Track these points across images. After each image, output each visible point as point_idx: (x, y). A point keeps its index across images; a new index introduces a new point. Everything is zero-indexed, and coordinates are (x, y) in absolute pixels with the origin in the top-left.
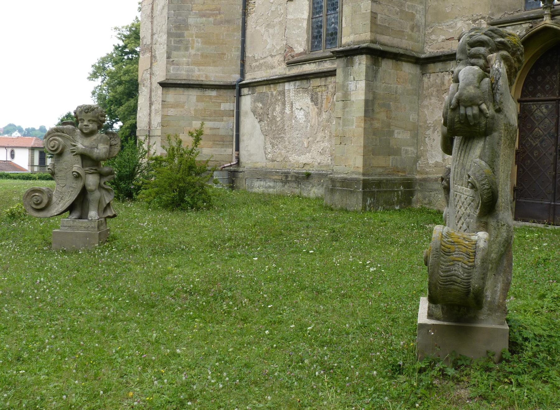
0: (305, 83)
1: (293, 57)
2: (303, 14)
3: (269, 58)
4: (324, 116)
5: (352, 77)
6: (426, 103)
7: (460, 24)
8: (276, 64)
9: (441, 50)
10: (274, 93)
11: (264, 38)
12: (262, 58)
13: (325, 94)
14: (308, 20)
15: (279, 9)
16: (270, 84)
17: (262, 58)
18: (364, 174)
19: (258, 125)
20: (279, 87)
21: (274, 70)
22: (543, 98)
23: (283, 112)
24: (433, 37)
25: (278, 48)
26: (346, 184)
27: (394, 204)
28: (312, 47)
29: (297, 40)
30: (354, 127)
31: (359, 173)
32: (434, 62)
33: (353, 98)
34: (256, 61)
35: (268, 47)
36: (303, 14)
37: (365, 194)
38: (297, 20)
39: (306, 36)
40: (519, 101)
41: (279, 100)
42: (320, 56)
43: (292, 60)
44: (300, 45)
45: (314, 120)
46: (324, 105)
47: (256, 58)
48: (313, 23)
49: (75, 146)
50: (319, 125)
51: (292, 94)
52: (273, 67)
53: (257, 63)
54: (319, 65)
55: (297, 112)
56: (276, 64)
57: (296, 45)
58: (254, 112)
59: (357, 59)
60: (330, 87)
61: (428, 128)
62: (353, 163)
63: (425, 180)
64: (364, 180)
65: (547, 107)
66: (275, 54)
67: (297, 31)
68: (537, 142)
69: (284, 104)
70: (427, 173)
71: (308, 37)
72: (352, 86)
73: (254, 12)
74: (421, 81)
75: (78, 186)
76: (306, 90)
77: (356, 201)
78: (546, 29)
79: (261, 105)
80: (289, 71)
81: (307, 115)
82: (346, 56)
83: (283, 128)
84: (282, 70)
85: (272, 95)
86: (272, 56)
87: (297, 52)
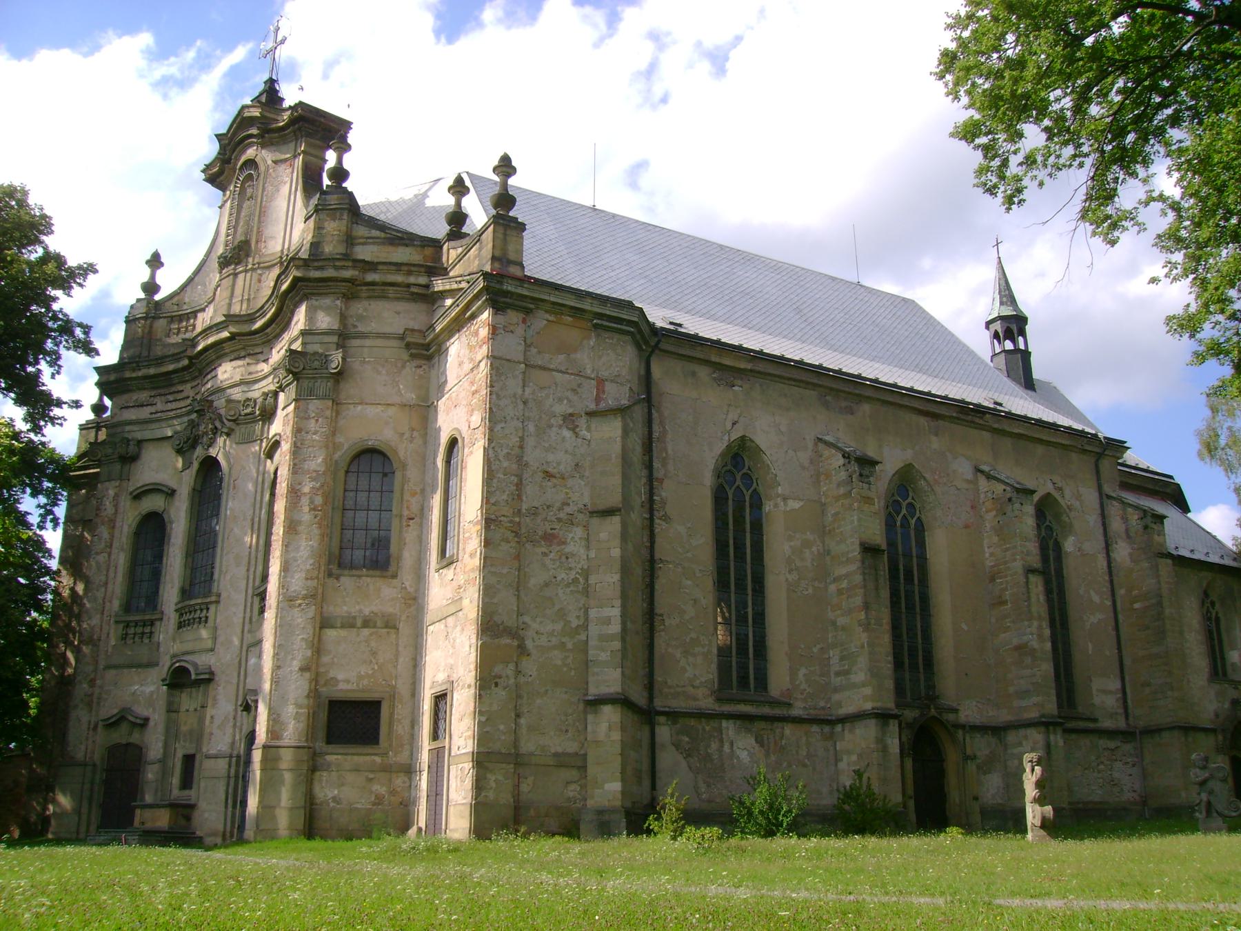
4: (773, 758)
10: (707, 728)
19: (684, 764)
20: (714, 723)
23: (720, 749)
25: (703, 680)
33: (891, 751)
55: (738, 752)
58: (677, 746)
59: (891, 721)
69: (721, 741)
72: (889, 741)
76: (748, 731)
81: (751, 755)
85: (704, 729)
86: (694, 687)
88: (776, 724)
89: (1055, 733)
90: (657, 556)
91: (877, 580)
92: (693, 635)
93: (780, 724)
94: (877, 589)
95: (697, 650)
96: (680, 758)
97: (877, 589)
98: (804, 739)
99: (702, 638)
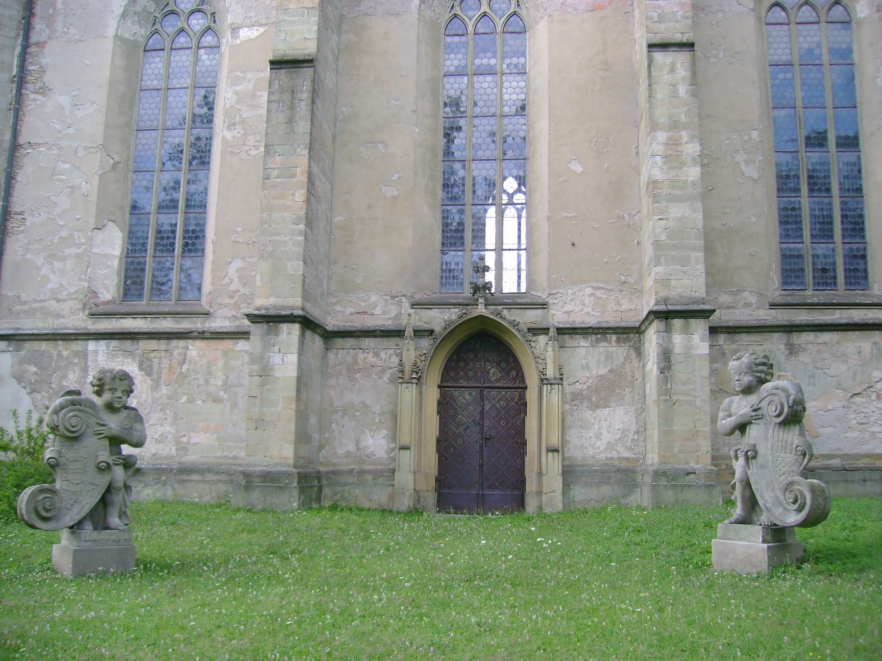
0: (128, 344)
1: (97, 305)
2: (114, 249)
3: (53, 303)
4: (164, 390)
5: (276, 348)
6: (332, 382)
7: (374, 298)
8: (67, 311)
9: (350, 324)
11: (43, 272)
12: (35, 301)
13: (166, 362)
14: (121, 259)
15: (76, 237)
16: (56, 340)
17: (35, 301)
18: (295, 466)
20: (78, 346)
21: (61, 320)
22: (465, 384)
24: (338, 308)
25: (73, 290)
26: (271, 479)
27: (657, 474)
28: (125, 295)
29: (104, 284)
30: (280, 409)
31: (288, 466)
32: (343, 337)
33: (278, 374)
34: (25, 303)
35: (50, 286)
36: (114, 249)
37: (302, 490)
38: (105, 256)
39: (116, 280)
40: (439, 387)
41: (75, 364)
42: (140, 310)
43: (95, 309)
44: (109, 290)
45: (144, 396)
46: (163, 376)
47: (23, 299)
49: (104, 425)
50: (153, 402)
51: (100, 358)
52: (58, 316)
53: (26, 307)
54: (151, 322)
56: (67, 311)
58: (19, 378)
59: (285, 327)
60: (176, 352)
61: (336, 412)
62: (280, 451)
63: (334, 472)
64: (299, 473)
65: (470, 394)
66: (65, 297)
67: (104, 272)
68: (461, 429)
70: (334, 465)
71: (120, 281)
72: (276, 358)
73: (23, 232)
74: (325, 357)
75: (103, 481)
77: (292, 499)
78: (481, 318)
79: (35, 369)
80: (93, 324)
82: (268, 322)
84: (79, 321)
85: (60, 355)
86: (58, 300)
88: (174, 343)
89: (686, 331)
90: (22, 139)
91: (292, 107)
92: (64, 233)
93: (182, 343)
94: (290, 121)
95: (68, 251)
96: (23, 394)
97: (290, 121)
98: (221, 363)
99: (76, 234)
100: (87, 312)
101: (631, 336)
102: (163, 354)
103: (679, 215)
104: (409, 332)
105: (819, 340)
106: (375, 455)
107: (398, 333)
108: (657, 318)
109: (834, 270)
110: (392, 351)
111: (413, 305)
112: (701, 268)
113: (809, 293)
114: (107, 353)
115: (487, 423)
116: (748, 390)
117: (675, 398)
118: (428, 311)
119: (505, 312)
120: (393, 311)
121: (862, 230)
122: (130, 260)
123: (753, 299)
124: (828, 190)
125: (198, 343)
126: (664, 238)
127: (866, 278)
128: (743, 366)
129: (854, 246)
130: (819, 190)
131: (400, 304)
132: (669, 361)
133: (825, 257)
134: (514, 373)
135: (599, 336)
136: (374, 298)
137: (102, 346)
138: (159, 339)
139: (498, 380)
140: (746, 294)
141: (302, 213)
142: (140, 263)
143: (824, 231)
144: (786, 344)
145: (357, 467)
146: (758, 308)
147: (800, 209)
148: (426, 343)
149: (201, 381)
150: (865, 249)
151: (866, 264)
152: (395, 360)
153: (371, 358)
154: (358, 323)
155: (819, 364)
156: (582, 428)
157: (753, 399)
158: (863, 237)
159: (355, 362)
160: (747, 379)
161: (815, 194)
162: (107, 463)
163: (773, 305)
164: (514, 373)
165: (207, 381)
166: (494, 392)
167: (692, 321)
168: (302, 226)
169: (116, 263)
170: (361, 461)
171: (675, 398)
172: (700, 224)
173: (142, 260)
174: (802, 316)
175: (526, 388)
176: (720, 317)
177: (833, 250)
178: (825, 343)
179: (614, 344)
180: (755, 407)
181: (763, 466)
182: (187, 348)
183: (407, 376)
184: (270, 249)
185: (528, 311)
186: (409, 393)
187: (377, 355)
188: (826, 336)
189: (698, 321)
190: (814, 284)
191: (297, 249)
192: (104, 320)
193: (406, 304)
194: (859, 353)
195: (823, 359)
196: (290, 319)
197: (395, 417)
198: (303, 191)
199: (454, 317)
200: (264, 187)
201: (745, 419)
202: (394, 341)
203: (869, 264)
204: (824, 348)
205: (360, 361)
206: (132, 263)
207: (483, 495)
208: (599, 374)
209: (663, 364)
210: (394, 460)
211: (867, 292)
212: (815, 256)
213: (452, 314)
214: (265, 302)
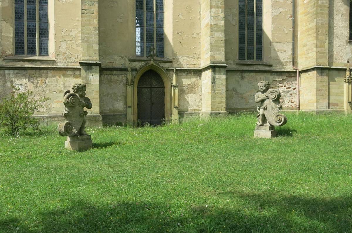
1: (6, 56)
2: (10, 34)
9: (108, 66)
14: (13, 38)
22: (145, 86)
29: (8, 48)
30: (94, 95)
32: (106, 70)
36: (10, 34)
38: (7, 37)
40: (137, 87)
48: (16, 40)
51: (11, 76)
57: (7, 50)
59: (94, 67)
65: (147, 90)
67: (7, 43)
70: (105, 113)
83: (5, 94)
87: (8, 54)
93: (45, 71)
100: (2, 59)
101: (198, 72)
102: (38, 75)
103: (218, 36)
104: (129, 69)
105: (250, 75)
106: (119, 109)
107: (126, 70)
108: (211, 68)
109: (253, 54)
110: (123, 76)
111: (129, 60)
112: (223, 52)
113: (246, 60)
114: (14, 75)
115: (153, 99)
116: (264, 92)
117: (216, 91)
118: (134, 63)
119: (159, 64)
120: (123, 62)
121: (261, 42)
122: (17, 39)
123: (232, 62)
124: (253, 29)
125: (52, 71)
126: (213, 43)
127: (262, 57)
128: (263, 84)
129: (259, 47)
130: (251, 29)
131: (125, 60)
132: (215, 81)
133: (251, 50)
134: (161, 83)
135: (188, 72)
136: (116, 57)
137: (11, 72)
138: (36, 70)
139: (155, 85)
140: (230, 60)
141: (97, 27)
142: (21, 40)
143: (251, 41)
144: (241, 76)
145: (112, 114)
146: (233, 65)
147: (245, 35)
148: (134, 73)
149: (54, 85)
150: (262, 48)
151: (262, 53)
152: (125, 78)
153: (116, 77)
154: (111, 66)
155: (250, 82)
156: (183, 100)
157: (265, 94)
158: (262, 44)
159: (111, 79)
160: (264, 88)
161: (249, 30)
162: (83, 114)
163: (238, 64)
164: (161, 83)
165: (56, 85)
166: (155, 89)
167: (221, 69)
168: (97, 32)
169: (11, 40)
170: (114, 111)
171: (216, 91)
172: (224, 39)
173: (22, 39)
174: (245, 68)
175: (165, 88)
176: (228, 68)
177: (253, 48)
178: (251, 76)
179: (193, 74)
180: (267, 95)
181: (269, 111)
182: (48, 73)
183: (129, 84)
184: (86, 39)
185: (166, 64)
186: (130, 89)
187: (118, 77)
188: (252, 74)
189: (223, 69)
190: (248, 58)
191: (96, 40)
192: (11, 62)
193: (127, 60)
194: (260, 79)
195: (251, 81)
196: (96, 64)
197: (126, 97)
198: (97, 19)
199: (143, 65)
200: (82, 17)
201: (264, 98)
202: (125, 72)
203: (263, 53)
204: (251, 77)
205: (113, 79)
206: (18, 40)
207: (152, 121)
208: (188, 84)
209: (213, 82)
210: (126, 111)
211: (262, 61)
212: (248, 50)
213: (143, 64)
214: (86, 59)
